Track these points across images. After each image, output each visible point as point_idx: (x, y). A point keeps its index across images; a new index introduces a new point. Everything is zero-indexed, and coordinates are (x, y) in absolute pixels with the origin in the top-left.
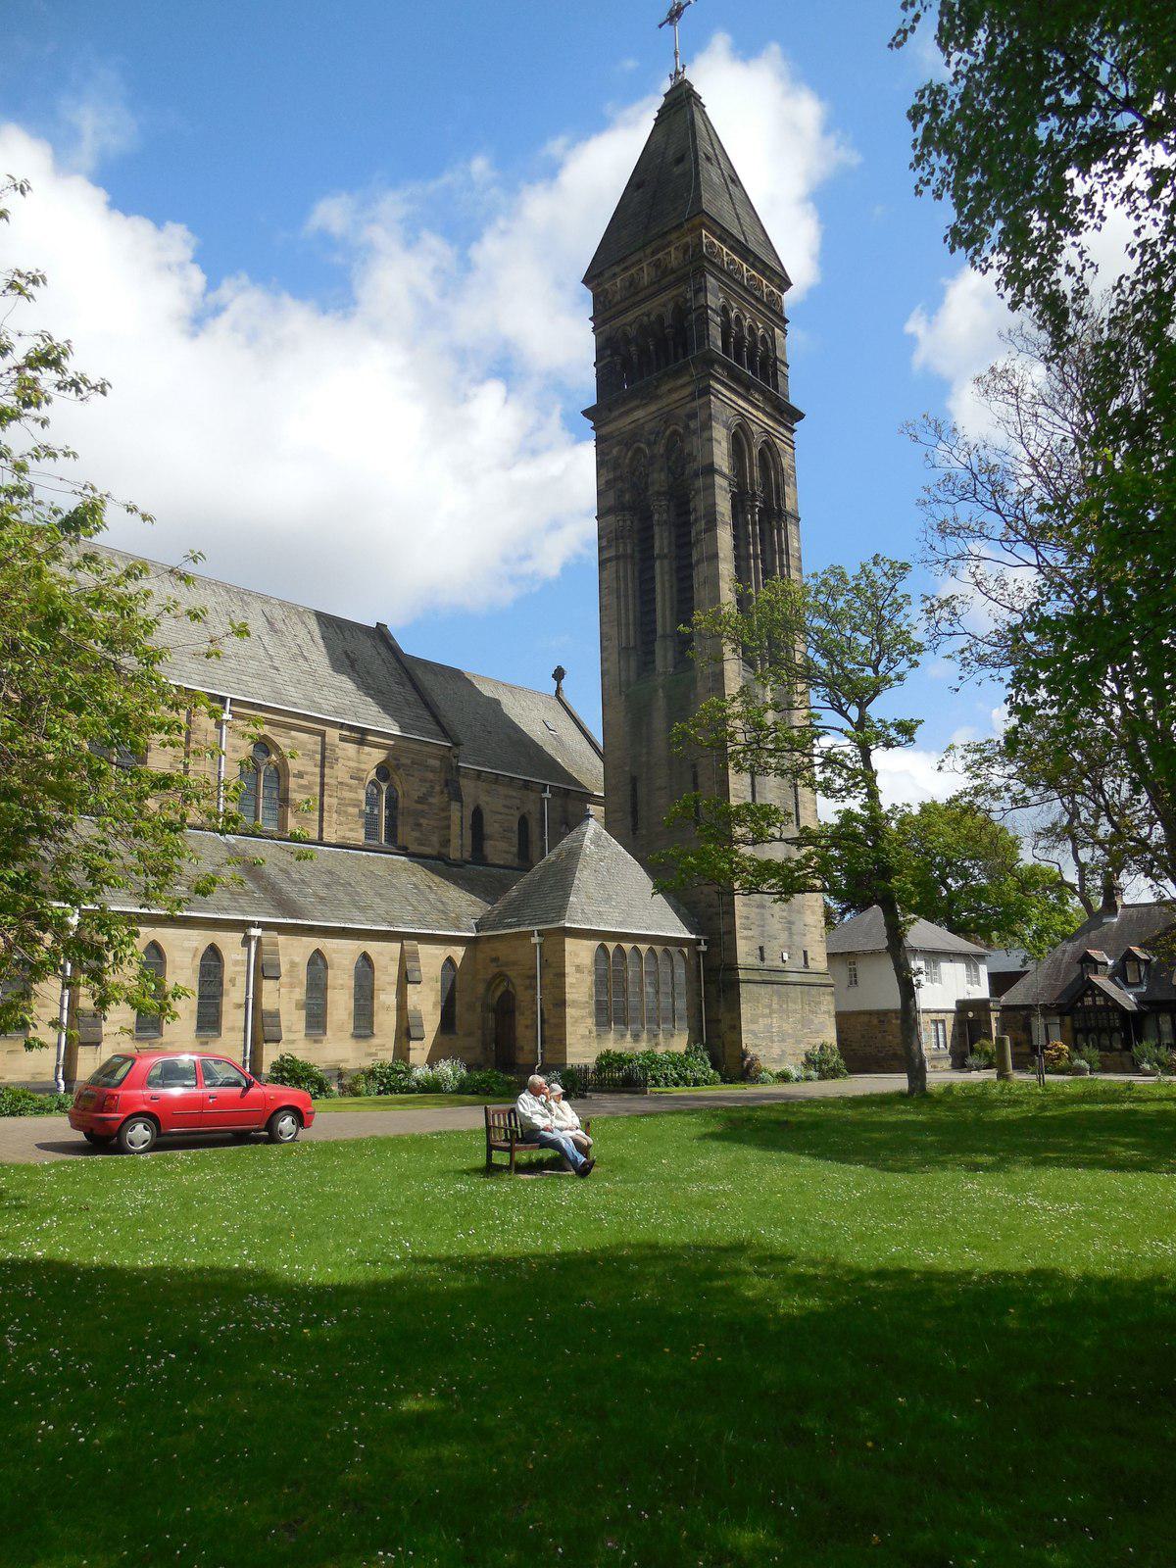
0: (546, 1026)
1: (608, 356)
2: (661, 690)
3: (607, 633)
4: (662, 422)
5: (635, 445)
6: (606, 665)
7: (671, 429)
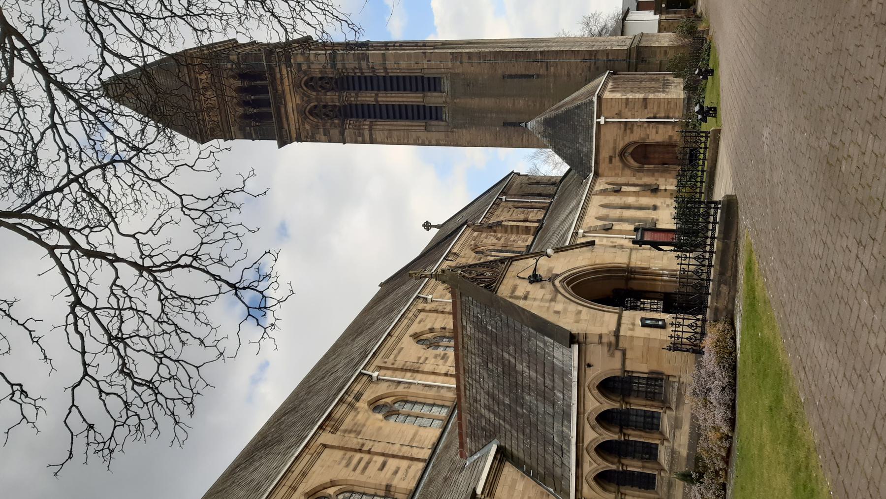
0: (658, 116)
2: (455, 101)
3: (414, 140)
5: (307, 113)
6: (433, 142)
7: (303, 85)
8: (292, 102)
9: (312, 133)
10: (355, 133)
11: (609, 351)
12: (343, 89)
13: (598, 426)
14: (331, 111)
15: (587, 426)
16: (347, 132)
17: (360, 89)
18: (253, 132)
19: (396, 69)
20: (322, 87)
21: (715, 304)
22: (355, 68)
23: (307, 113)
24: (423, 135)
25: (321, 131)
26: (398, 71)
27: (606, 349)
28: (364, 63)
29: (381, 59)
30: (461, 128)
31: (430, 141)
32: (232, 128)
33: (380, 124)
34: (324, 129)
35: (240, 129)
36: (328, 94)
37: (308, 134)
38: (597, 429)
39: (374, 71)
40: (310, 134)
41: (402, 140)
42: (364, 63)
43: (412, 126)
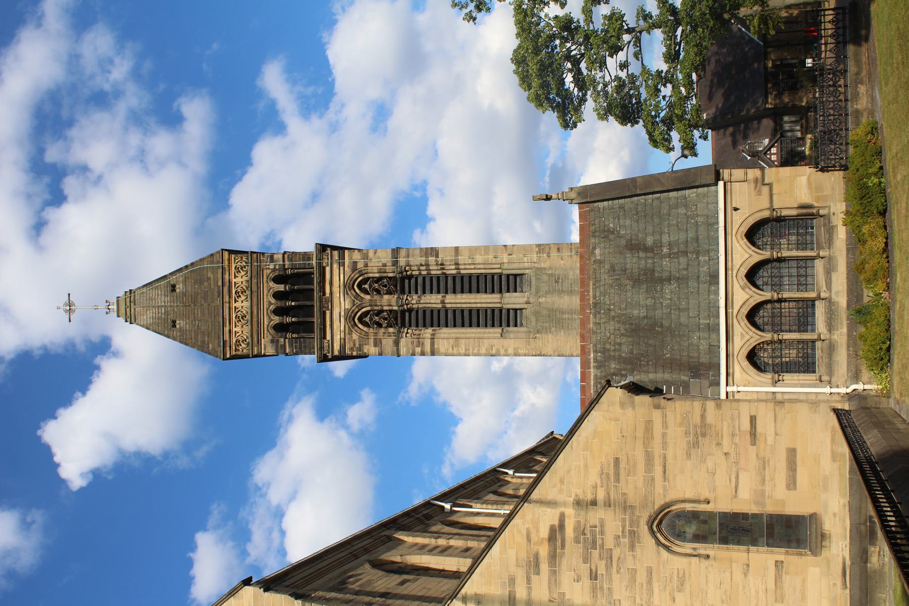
1: (285, 341)
2: (540, 300)
3: (486, 350)
4: (349, 292)
8: (341, 304)
9: (360, 345)
10: (412, 343)
11: (755, 188)
12: (403, 292)
13: (749, 284)
14: (385, 319)
15: (737, 286)
16: (403, 342)
17: (424, 292)
18: (287, 344)
19: (470, 264)
20: (378, 292)
21: (855, 106)
22: (421, 265)
24: (498, 343)
25: (372, 341)
26: (473, 267)
27: (752, 185)
28: (432, 260)
29: (453, 253)
30: (546, 332)
31: (506, 350)
32: (262, 340)
33: (444, 332)
35: (272, 341)
36: (386, 297)
37: (354, 345)
38: (747, 290)
39: (443, 269)
40: (357, 345)
41: (471, 350)
42: (432, 260)
43: (485, 333)
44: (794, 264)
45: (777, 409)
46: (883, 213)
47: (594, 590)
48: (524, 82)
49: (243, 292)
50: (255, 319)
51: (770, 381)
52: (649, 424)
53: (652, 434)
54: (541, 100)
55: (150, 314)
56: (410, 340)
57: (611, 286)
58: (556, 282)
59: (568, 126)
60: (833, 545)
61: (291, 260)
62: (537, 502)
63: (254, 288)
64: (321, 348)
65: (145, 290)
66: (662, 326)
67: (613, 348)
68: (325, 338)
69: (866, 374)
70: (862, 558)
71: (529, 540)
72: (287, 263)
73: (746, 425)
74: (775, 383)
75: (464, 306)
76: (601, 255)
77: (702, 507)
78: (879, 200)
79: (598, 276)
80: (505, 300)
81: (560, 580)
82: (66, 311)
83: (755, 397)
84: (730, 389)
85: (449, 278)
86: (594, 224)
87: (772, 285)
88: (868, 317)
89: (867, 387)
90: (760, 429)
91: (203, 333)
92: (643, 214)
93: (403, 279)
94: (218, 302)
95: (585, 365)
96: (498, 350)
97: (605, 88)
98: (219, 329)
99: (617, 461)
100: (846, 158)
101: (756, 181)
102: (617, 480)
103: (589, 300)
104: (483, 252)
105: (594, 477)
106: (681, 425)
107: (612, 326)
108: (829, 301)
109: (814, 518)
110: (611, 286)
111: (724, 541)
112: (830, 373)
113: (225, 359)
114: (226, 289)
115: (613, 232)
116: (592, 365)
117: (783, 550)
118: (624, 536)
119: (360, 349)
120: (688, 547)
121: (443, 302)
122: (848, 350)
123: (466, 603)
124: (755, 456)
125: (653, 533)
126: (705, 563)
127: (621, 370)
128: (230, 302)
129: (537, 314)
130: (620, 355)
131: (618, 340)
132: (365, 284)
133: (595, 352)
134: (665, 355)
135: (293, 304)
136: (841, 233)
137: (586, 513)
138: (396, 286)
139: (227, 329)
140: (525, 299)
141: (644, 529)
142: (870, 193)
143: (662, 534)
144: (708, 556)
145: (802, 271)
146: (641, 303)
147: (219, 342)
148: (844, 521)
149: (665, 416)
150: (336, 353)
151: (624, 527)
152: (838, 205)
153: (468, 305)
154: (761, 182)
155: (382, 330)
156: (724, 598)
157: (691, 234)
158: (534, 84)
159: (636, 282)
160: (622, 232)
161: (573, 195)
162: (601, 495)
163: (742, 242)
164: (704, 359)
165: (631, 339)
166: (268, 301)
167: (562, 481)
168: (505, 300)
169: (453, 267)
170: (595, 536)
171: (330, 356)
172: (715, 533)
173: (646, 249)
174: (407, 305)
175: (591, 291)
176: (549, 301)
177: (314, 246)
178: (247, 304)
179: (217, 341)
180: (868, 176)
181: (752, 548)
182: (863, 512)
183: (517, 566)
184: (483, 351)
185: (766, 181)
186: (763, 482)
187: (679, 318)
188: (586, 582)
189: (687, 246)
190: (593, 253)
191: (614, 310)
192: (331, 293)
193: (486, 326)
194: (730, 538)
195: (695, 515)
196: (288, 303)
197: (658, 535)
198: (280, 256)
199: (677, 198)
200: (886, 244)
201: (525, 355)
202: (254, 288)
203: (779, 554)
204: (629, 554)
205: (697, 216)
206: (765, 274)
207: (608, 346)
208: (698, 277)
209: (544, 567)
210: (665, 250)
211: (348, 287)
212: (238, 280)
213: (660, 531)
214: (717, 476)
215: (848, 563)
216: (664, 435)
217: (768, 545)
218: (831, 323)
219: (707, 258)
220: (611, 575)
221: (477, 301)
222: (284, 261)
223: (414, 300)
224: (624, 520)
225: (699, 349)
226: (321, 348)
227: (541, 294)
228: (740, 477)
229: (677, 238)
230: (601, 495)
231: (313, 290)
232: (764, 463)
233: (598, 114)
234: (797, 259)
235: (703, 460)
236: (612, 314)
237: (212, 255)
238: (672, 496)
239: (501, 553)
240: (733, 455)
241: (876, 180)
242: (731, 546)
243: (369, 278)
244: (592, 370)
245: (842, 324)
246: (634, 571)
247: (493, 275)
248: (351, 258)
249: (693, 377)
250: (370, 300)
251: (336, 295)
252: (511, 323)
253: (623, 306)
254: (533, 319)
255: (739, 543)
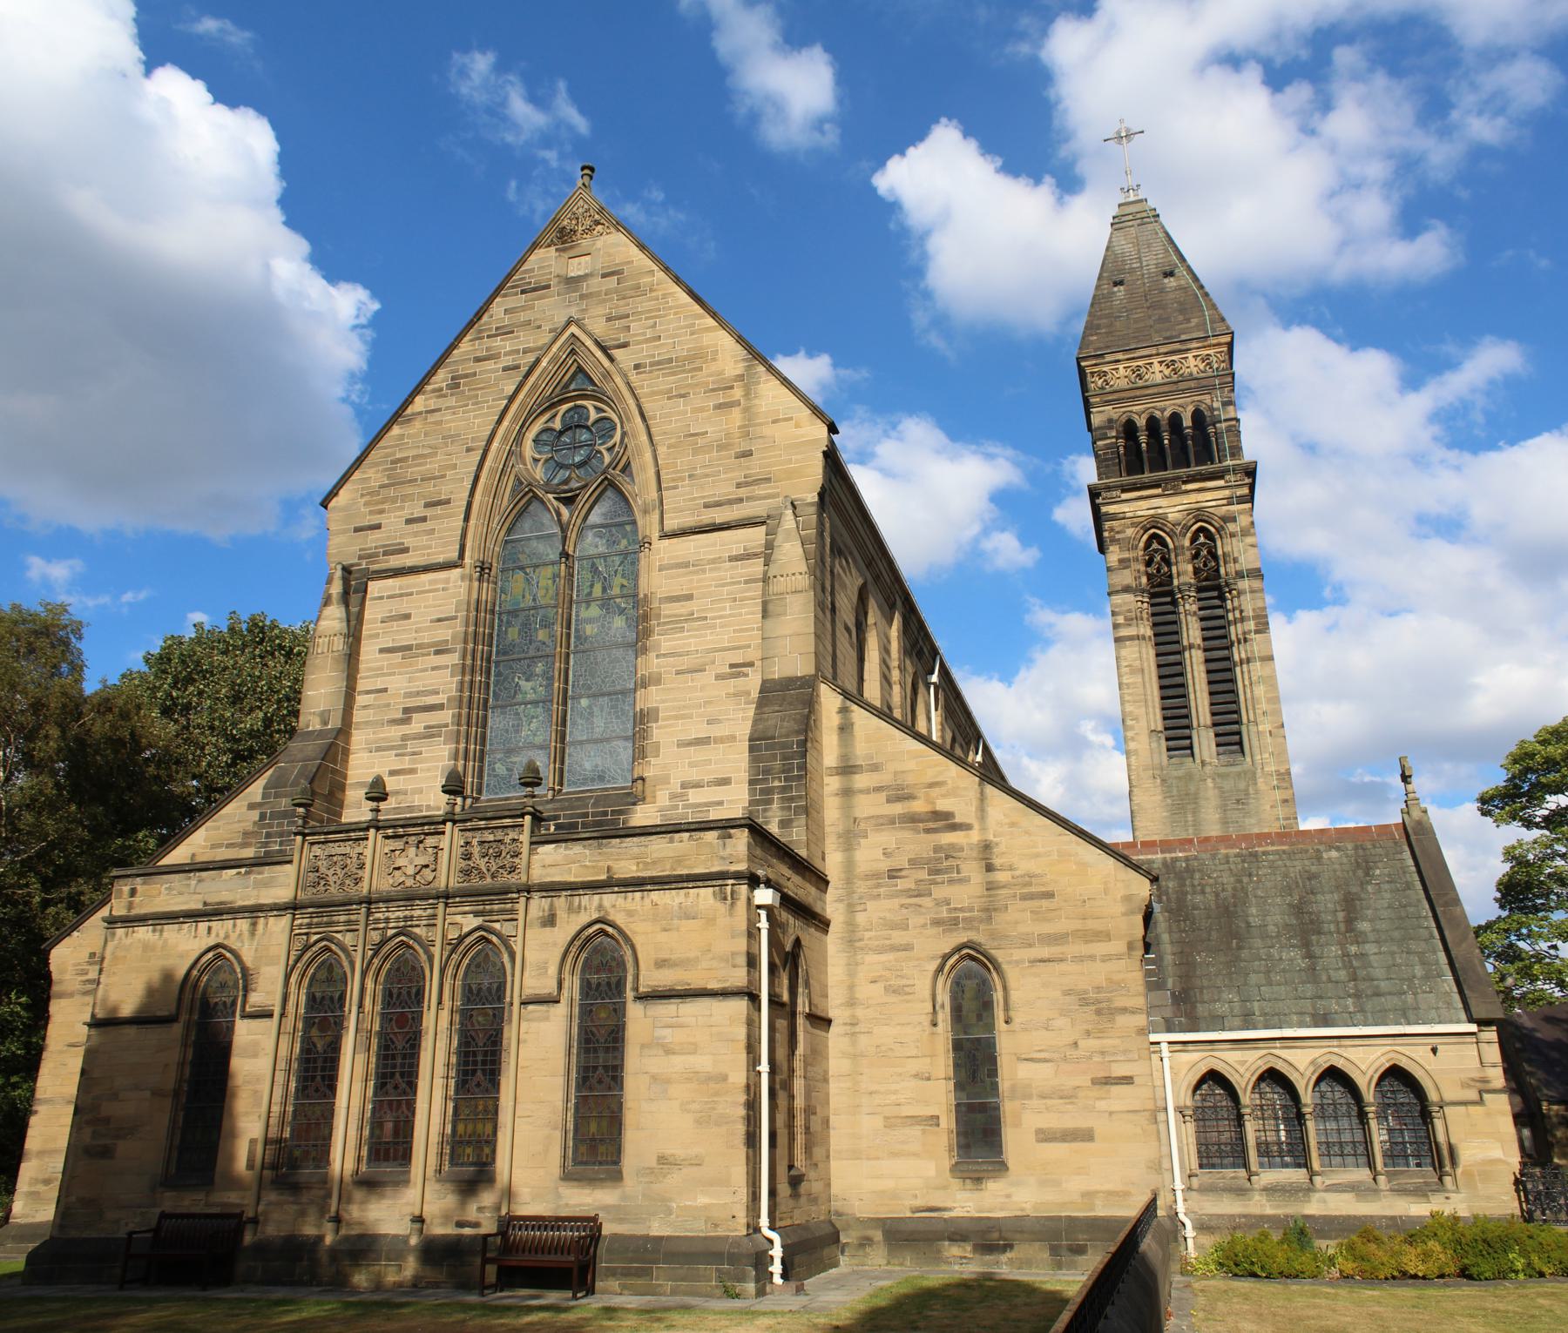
2: (1209, 780)
5: (1152, 531)
8: (1173, 507)
10: (1129, 611)
11: (1473, 1080)
12: (1199, 590)
13: (1320, 1071)
14: (1158, 570)
15: (1316, 1053)
16: (1129, 597)
17: (1202, 619)
18: (1108, 441)
20: (1196, 556)
22: (1241, 612)
23: (1152, 531)
25: (1126, 555)
26: (1247, 683)
27: (1476, 1075)
28: (1251, 625)
29: (1263, 654)
31: (1133, 739)
34: (1129, 560)
36: (1190, 568)
37: (1118, 532)
38: (1312, 1069)
39: (1239, 642)
40: (1117, 536)
41: (1130, 691)
42: (1251, 625)
43: (1154, 707)
44: (1359, 1136)
45: (1147, 1114)
46: (1465, 1274)
47: (875, 875)
48: (1551, 734)
49: (1175, 371)
50: (1138, 393)
51: (1182, 1104)
52: (1105, 936)
53: (1092, 941)
54: (1523, 761)
55: (1128, 248)
56: (1133, 606)
57: (1286, 876)
58: (1238, 801)
59: (1483, 804)
60: (967, 1195)
61: (1229, 429)
62: (982, 793)
63: (1182, 386)
64: (1109, 488)
65: (1161, 235)
66: (1240, 948)
67: (1196, 883)
68: (1124, 491)
69: (1208, 1241)
70: (955, 1233)
71: (932, 785)
72: (1224, 425)
73: (1119, 1070)
74: (1180, 1111)
75: (1189, 676)
76: (1329, 859)
77: (999, 1014)
78: (1486, 1267)
79: (1297, 856)
80: (1203, 732)
81: (883, 830)
82: (1119, 132)
83: (1158, 1083)
84: (1164, 1046)
85: (1226, 652)
86: (1374, 847)
87: (1322, 1105)
88: (1295, 1245)
89: (1190, 1242)
90: (1116, 1089)
91: (1111, 325)
92: (1403, 914)
93: (1218, 588)
94: (1157, 339)
95: (1166, 846)
96: (1132, 728)
97: (1559, 856)
98: (1118, 346)
99: (1049, 895)
100: (1545, 1221)
101: (1485, 1081)
102: (1024, 898)
103: (1260, 845)
104: (1270, 695)
105: (1024, 866)
106: (1110, 980)
107: (1228, 880)
108: (1310, 1188)
109: (1002, 1167)
110: (1286, 876)
111: (957, 1046)
112: (1203, 1190)
113: (1079, 360)
114: (1177, 346)
115: (1367, 874)
116: (1168, 856)
117: (953, 1126)
118: (950, 911)
119: (1113, 540)
120: (944, 997)
121: (1191, 647)
122: (1240, 1216)
123: (839, 712)
124: (1077, 1083)
125: (958, 949)
126: (926, 1020)
127: (1167, 894)
128: (1158, 354)
129: (1189, 777)
130: (1187, 893)
131: (1208, 889)
132: (1206, 537)
133: (1187, 859)
134: (1199, 955)
135: (1166, 442)
136: (1418, 1209)
137: (975, 859)
138: (1206, 579)
139: (1120, 356)
140: (1208, 760)
141: (963, 938)
142: (1496, 1255)
143: (958, 961)
144: (935, 1025)
145: (1348, 1149)
146: (1269, 918)
147: (1100, 349)
148: (1002, 1210)
149: (1119, 957)
150: (1104, 509)
151: (961, 910)
152: (1464, 1206)
153: (1190, 682)
154: (1484, 1089)
155: (1142, 568)
156: (883, 1048)
157: (1384, 986)
158: (1550, 749)
159: (1299, 910)
160: (1370, 888)
161: (1416, 814)
162: (1001, 877)
163: (1383, 1060)
164: (1201, 1010)
165: (1213, 906)
166: (1165, 408)
167: (1013, 825)
168: (1203, 732)
169: (1243, 656)
170: (946, 873)
171: (1100, 501)
172: (966, 1033)
173: (1350, 922)
174: (1182, 598)
175: (1274, 848)
176: (1210, 791)
177: (1253, 459)
178: (1158, 378)
179: (1102, 345)
180: (1524, 1253)
181: (952, 1083)
182: (1018, 1236)
183: (896, 773)
184: (1129, 708)
185: (1486, 1096)
186: (1043, 1097)
187: (1254, 972)
188: (885, 865)
189: (1364, 979)
190: (1331, 848)
191: (1251, 881)
192: (1187, 492)
193: (1163, 709)
194: (962, 1053)
195: (988, 1005)
196: (1166, 435)
197: (956, 957)
198: (1232, 415)
199: (1437, 963)
200: (1415, 1277)
201: (1129, 765)
202: (1182, 386)
203: (948, 1122)
204: (926, 919)
205: (1415, 994)
206: (1337, 1095)
207: (1197, 876)
208: (1321, 998)
209: (898, 809)
210: (1353, 949)
211: (1199, 514)
212: (1192, 362)
213: (962, 958)
214: (1044, 1032)
215: (947, 1215)
216: (1092, 958)
217: (958, 1105)
218: (1276, 1191)
219: (1351, 1009)
220: (897, 897)
221: (1198, 694)
222: (1226, 420)
223: (1189, 607)
224: (971, 909)
225: (1215, 1001)
226: (1109, 488)
227: (1218, 780)
228: (1049, 1064)
229: (1375, 965)
230: (1001, 877)
231: (1189, 466)
232: (1069, 1096)
233: (1514, 847)
234: (1367, 1143)
235: (1064, 1013)
236: (1245, 880)
237: (1223, 320)
238: (1011, 973)
239: (908, 752)
240: (1075, 1053)
241: (1519, 1265)
242: (951, 1055)
243: (1214, 540)
244: (1160, 856)
245: (1278, 1207)
246: (904, 926)
247: (1237, 712)
248: (1240, 513)
249: (1173, 994)
250: (1183, 547)
251: (1185, 499)
252: (1171, 743)
253: (1260, 893)
254: (1180, 773)
255: (956, 1066)
